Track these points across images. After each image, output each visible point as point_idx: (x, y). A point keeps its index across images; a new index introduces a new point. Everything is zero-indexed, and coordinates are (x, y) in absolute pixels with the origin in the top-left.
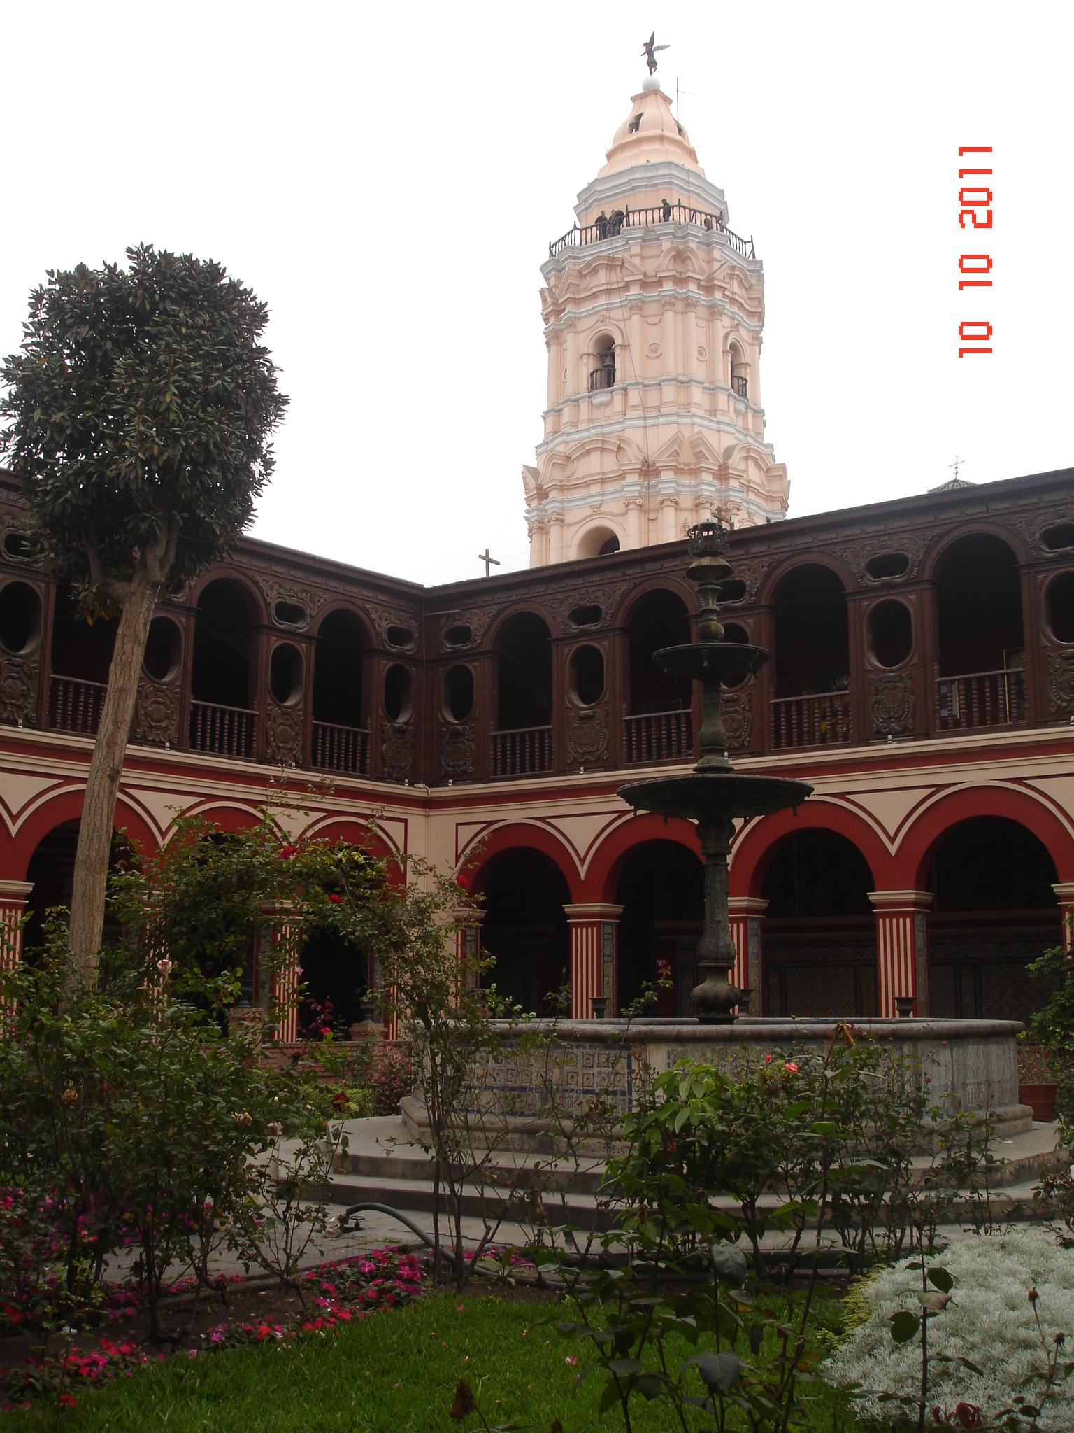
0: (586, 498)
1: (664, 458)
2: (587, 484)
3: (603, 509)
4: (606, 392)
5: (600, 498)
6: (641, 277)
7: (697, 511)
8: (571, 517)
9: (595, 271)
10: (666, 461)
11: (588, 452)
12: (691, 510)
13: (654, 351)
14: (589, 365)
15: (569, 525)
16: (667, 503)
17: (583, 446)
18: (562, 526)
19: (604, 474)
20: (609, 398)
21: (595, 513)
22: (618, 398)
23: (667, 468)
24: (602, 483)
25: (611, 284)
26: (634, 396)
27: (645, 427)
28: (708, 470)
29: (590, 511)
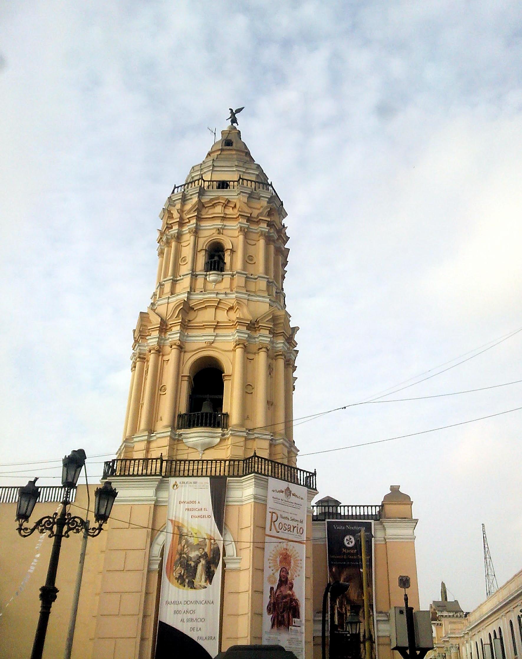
4: (219, 275)
6: (249, 215)
7: (276, 360)
9: (214, 206)
11: (206, 307)
13: (250, 260)
14: (202, 259)
15: (185, 352)
16: (264, 349)
19: (218, 322)
22: (227, 279)
23: (265, 328)
24: (215, 329)
25: (226, 214)
27: (248, 300)
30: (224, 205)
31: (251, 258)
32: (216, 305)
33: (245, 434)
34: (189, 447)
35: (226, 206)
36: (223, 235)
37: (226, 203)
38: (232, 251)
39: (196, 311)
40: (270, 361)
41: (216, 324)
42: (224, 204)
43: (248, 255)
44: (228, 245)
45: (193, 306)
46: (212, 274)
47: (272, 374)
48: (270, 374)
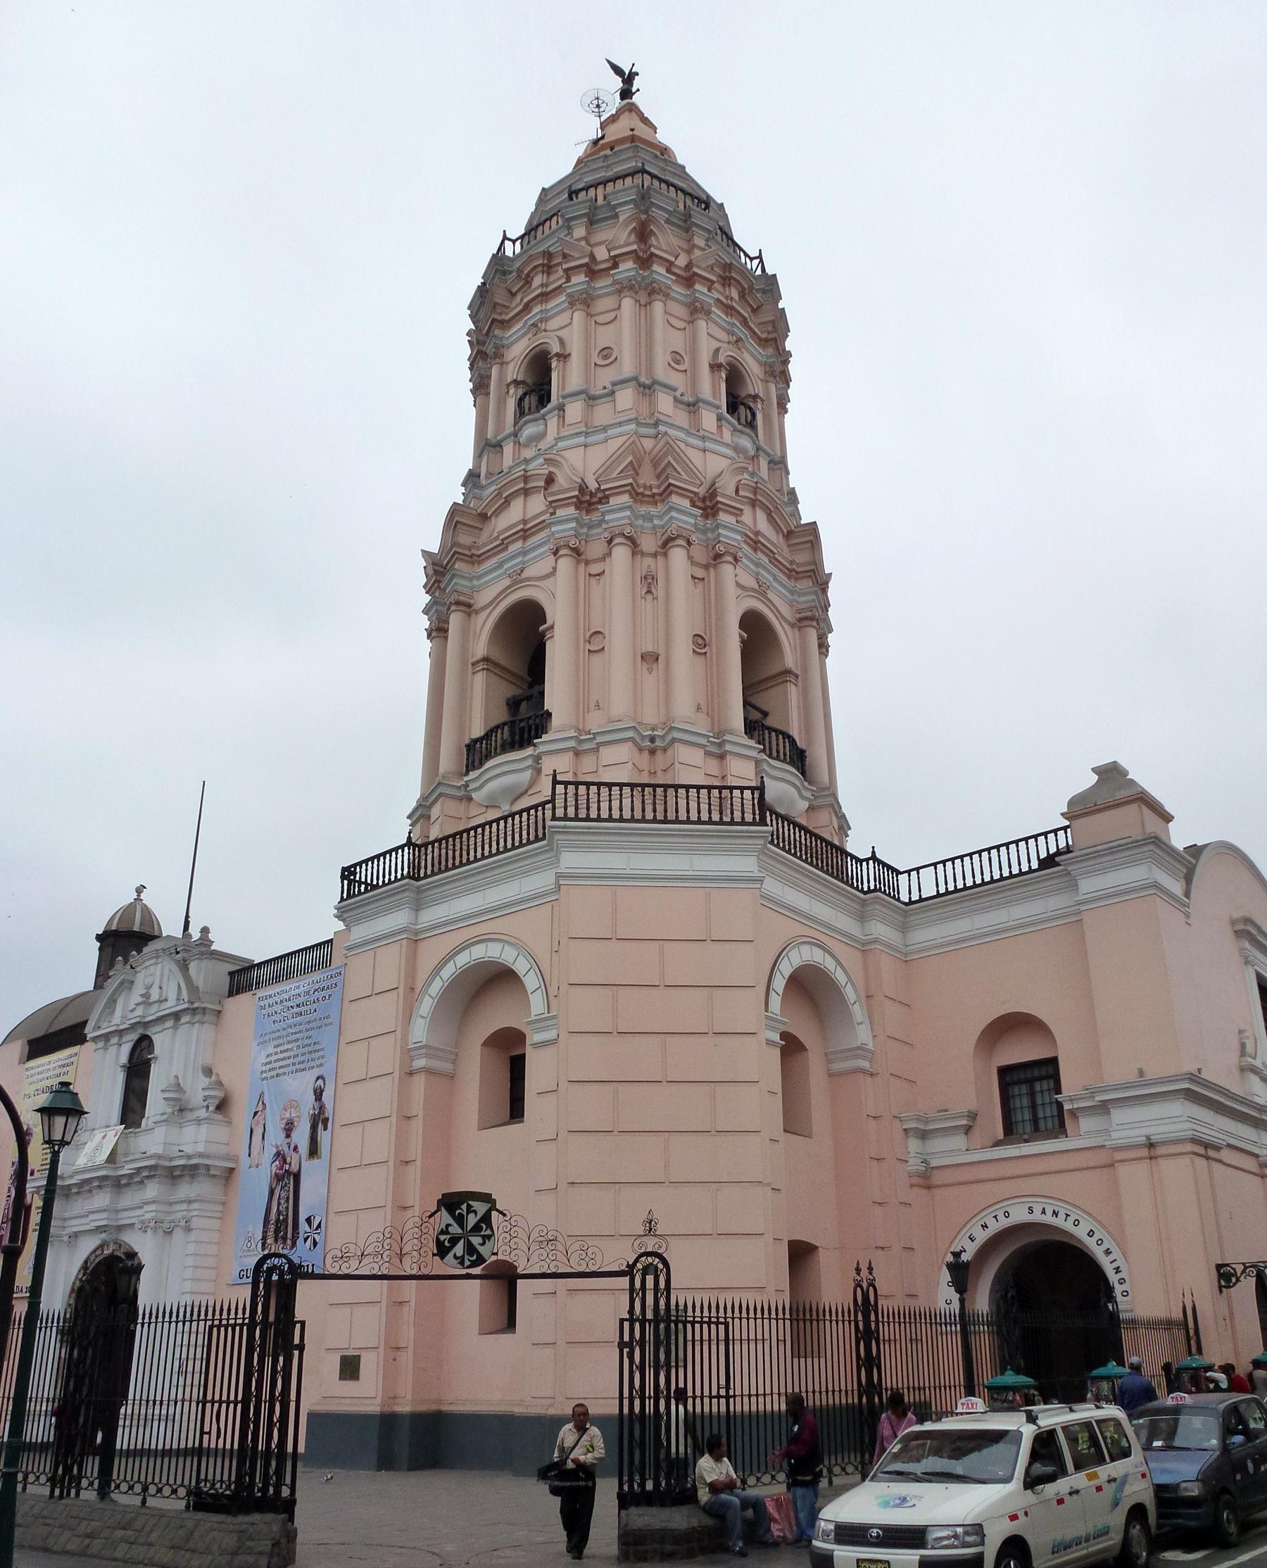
0: (501, 565)
1: (614, 475)
2: (504, 546)
3: (524, 575)
4: (536, 420)
5: (520, 559)
6: (586, 260)
7: (665, 555)
8: (483, 598)
10: (616, 479)
11: (507, 502)
12: (655, 555)
13: (606, 357)
15: (477, 612)
16: (617, 540)
17: (500, 493)
18: (469, 615)
20: (542, 427)
21: (515, 583)
23: (618, 491)
26: (575, 411)
28: (683, 492)
29: (507, 582)
30: (545, 268)
31: (605, 352)
32: (522, 485)
33: (572, 744)
34: (487, 807)
35: (550, 267)
36: (547, 333)
37: (546, 262)
38: (564, 357)
39: (493, 520)
40: (648, 561)
41: (521, 527)
42: (543, 265)
43: (599, 349)
44: (555, 348)
45: (483, 509)
46: (523, 426)
47: (653, 590)
48: (649, 592)
